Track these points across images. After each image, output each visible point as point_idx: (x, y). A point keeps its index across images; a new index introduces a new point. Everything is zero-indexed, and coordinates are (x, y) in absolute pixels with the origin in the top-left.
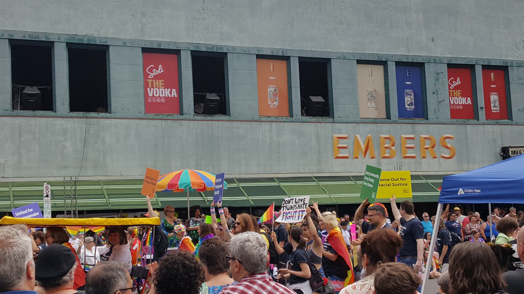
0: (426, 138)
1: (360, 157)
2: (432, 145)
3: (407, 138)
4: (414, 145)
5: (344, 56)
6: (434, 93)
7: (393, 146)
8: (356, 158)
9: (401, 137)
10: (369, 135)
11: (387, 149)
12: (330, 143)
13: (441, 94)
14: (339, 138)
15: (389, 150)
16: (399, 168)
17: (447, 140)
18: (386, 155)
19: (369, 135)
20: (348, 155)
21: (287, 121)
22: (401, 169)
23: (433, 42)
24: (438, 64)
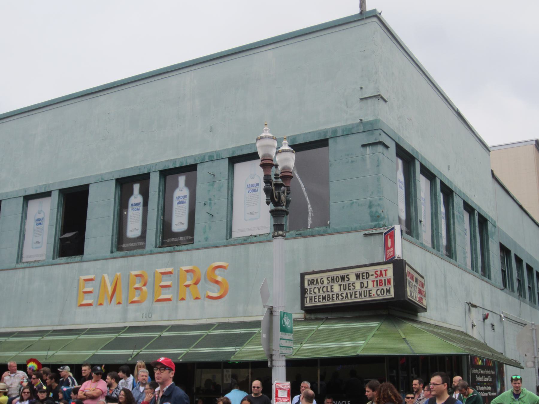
0: (187, 271)
1: (105, 304)
2: (195, 281)
3: (163, 273)
4: (171, 282)
5: (102, 179)
6: (205, 204)
7: (145, 285)
8: (101, 304)
9: (154, 273)
10: (118, 274)
11: (137, 290)
12: (75, 288)
13: (215, 204)
14: (86, 280)
15: (139, 292)
16: (149, 315)
17: (217, 271)
18: (136, 299)
19: (118, 274)
20: (93, 302)
21: (38, 265)
22: (151, 317)
23: (211, 133)
24: (216, 161)
